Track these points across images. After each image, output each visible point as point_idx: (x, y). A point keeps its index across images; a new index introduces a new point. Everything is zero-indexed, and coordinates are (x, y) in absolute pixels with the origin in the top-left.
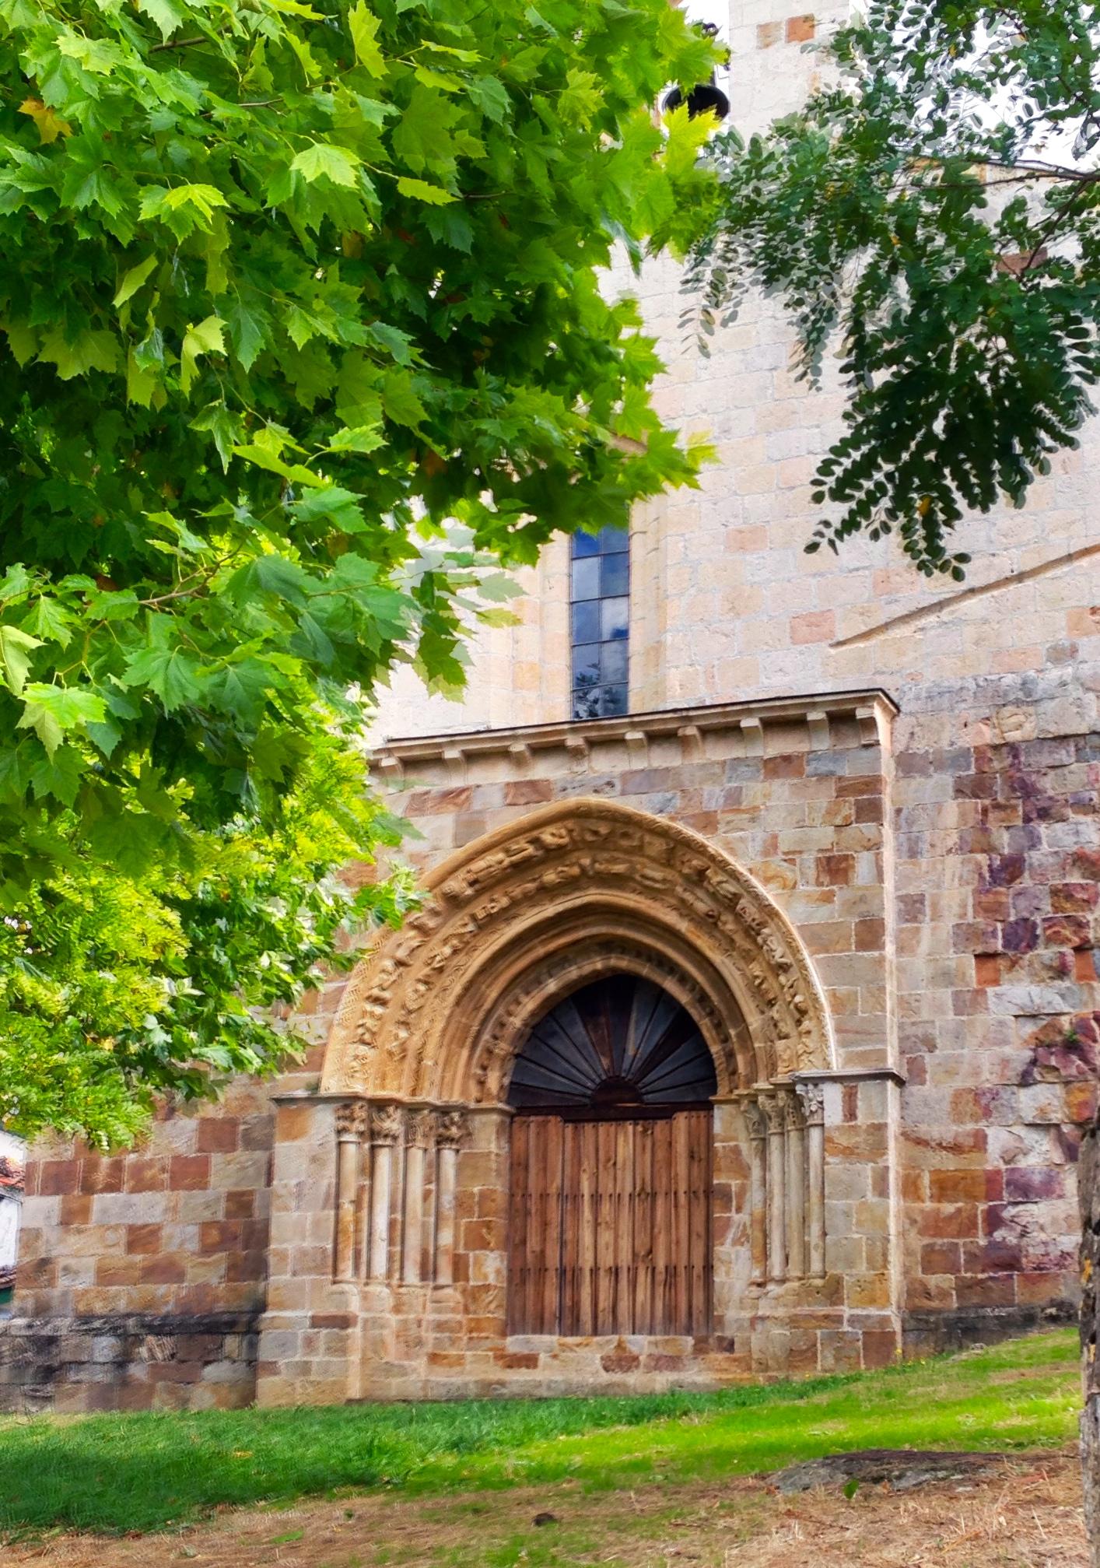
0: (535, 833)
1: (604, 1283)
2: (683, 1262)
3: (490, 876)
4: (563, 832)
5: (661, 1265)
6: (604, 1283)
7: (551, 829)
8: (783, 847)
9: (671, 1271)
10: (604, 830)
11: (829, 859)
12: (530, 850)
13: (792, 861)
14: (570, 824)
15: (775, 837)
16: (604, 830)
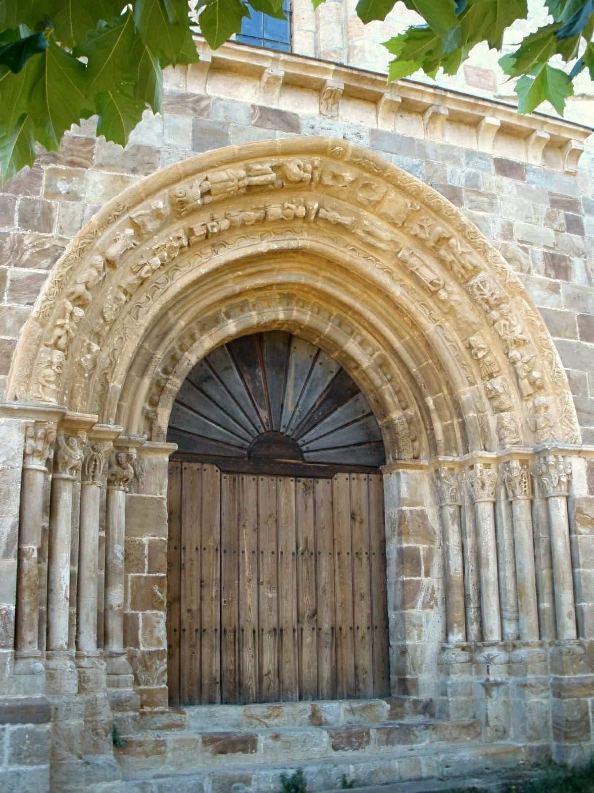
0: (282, 160)
1: (268, 641)
2: (349, 623)
3: (223, 190)
4: (309, 167)
5: (326, 626)
6: (268, 641)
7: (298, 160)
8: (517, 235)
9: (335, 630)
10: (349, 176)
11: (553, 256)
12: (272, 176)
13: (525, 250)
14: (317, 160)
15: (510, 225)
16: (349, 176)
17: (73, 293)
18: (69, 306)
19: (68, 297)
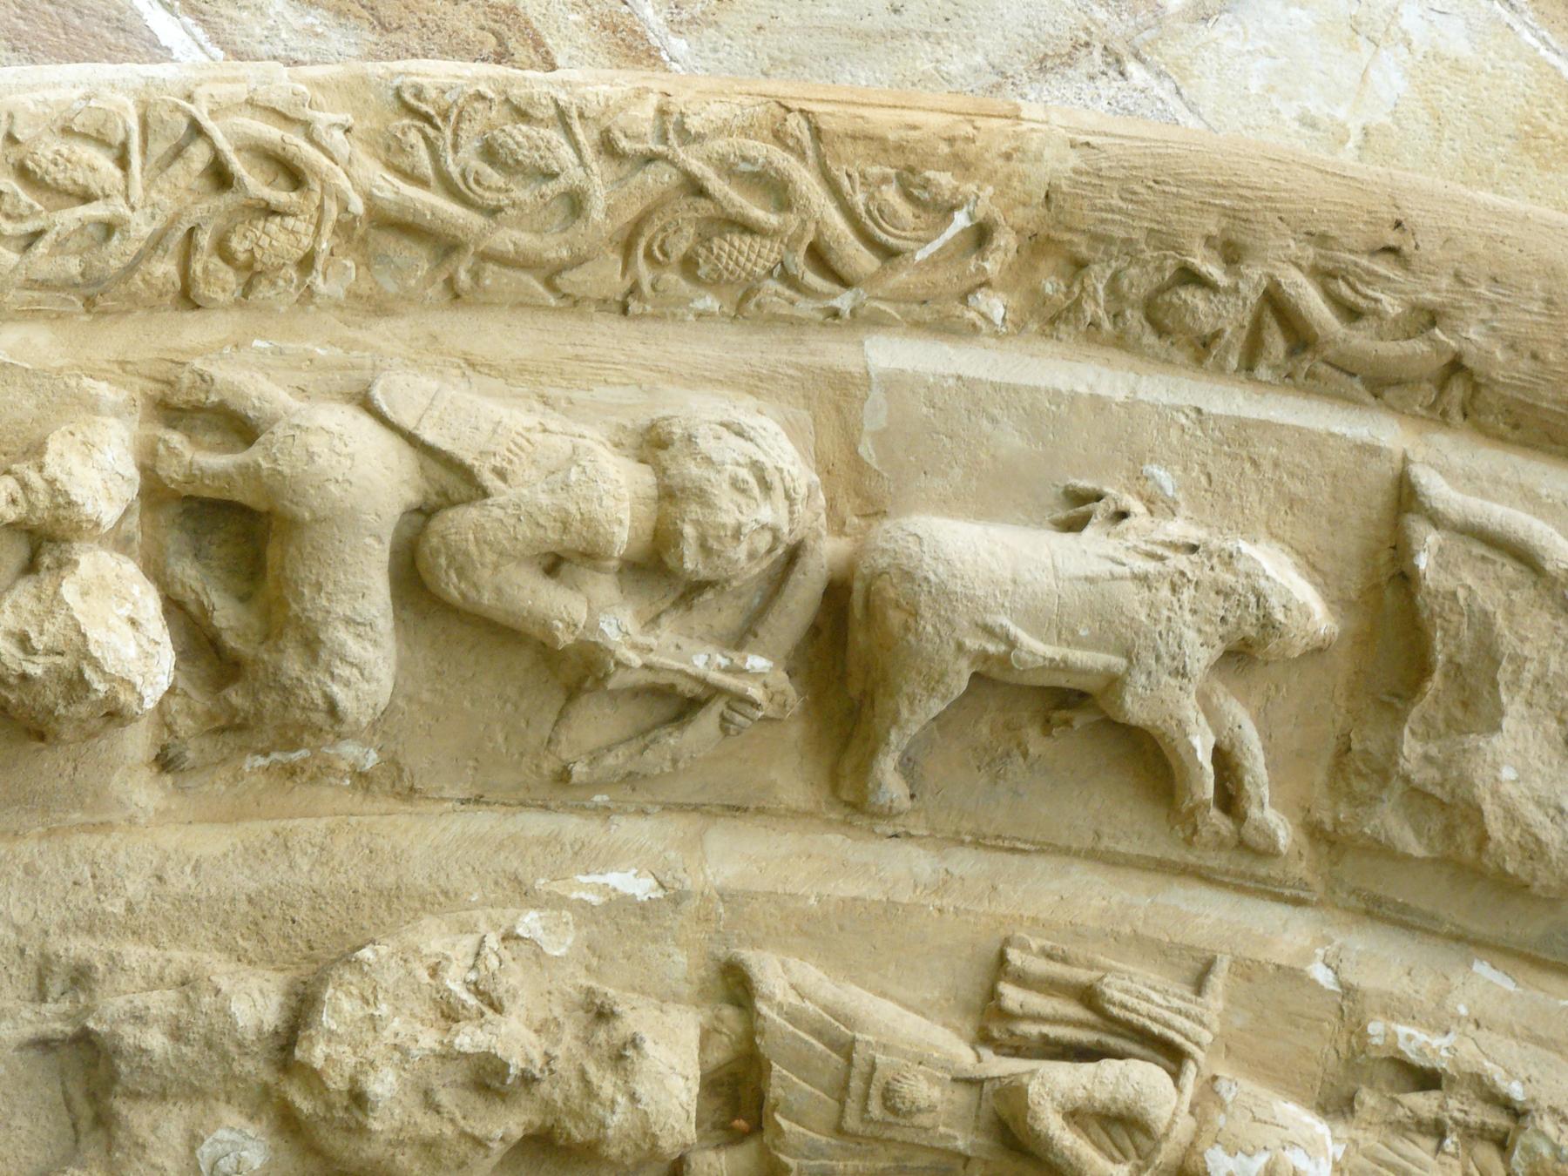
17: (239, 427)
18: (98, 469)
19: (174, 409)
